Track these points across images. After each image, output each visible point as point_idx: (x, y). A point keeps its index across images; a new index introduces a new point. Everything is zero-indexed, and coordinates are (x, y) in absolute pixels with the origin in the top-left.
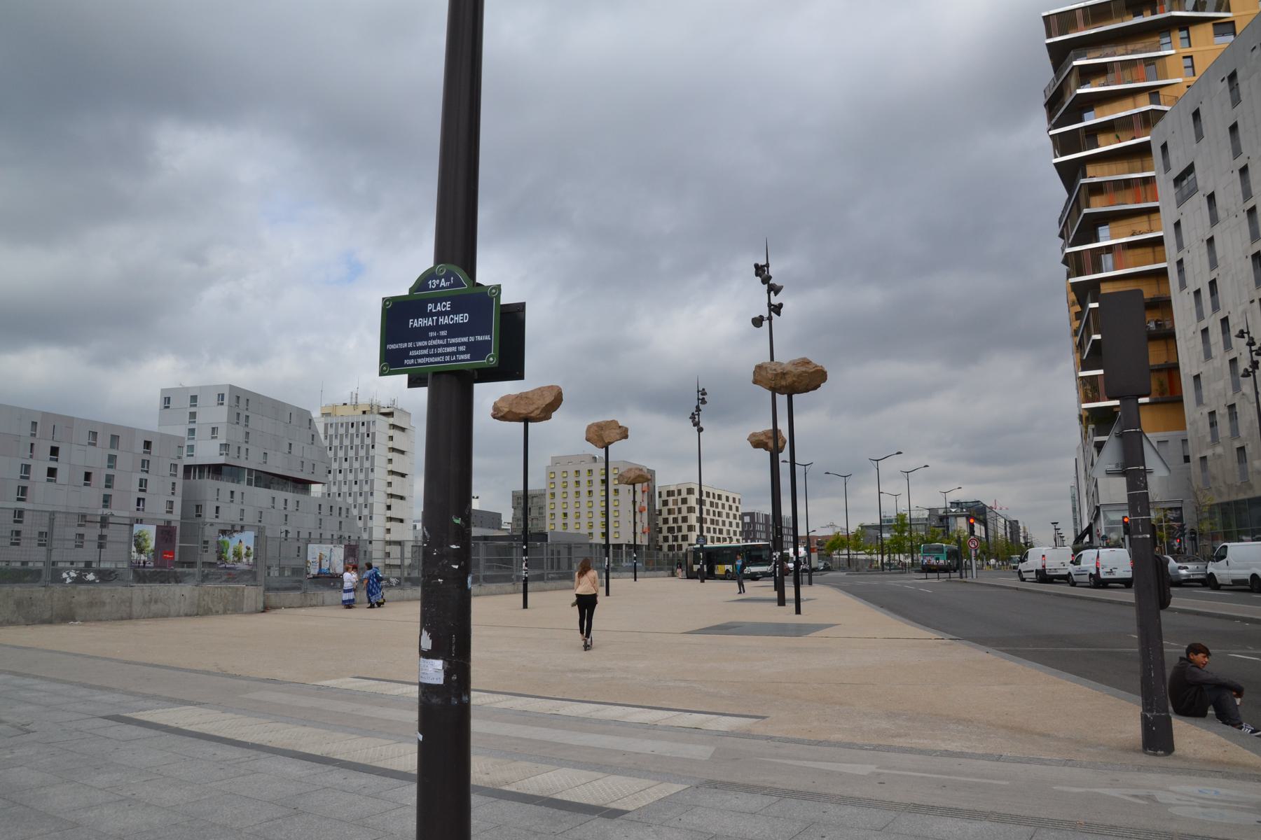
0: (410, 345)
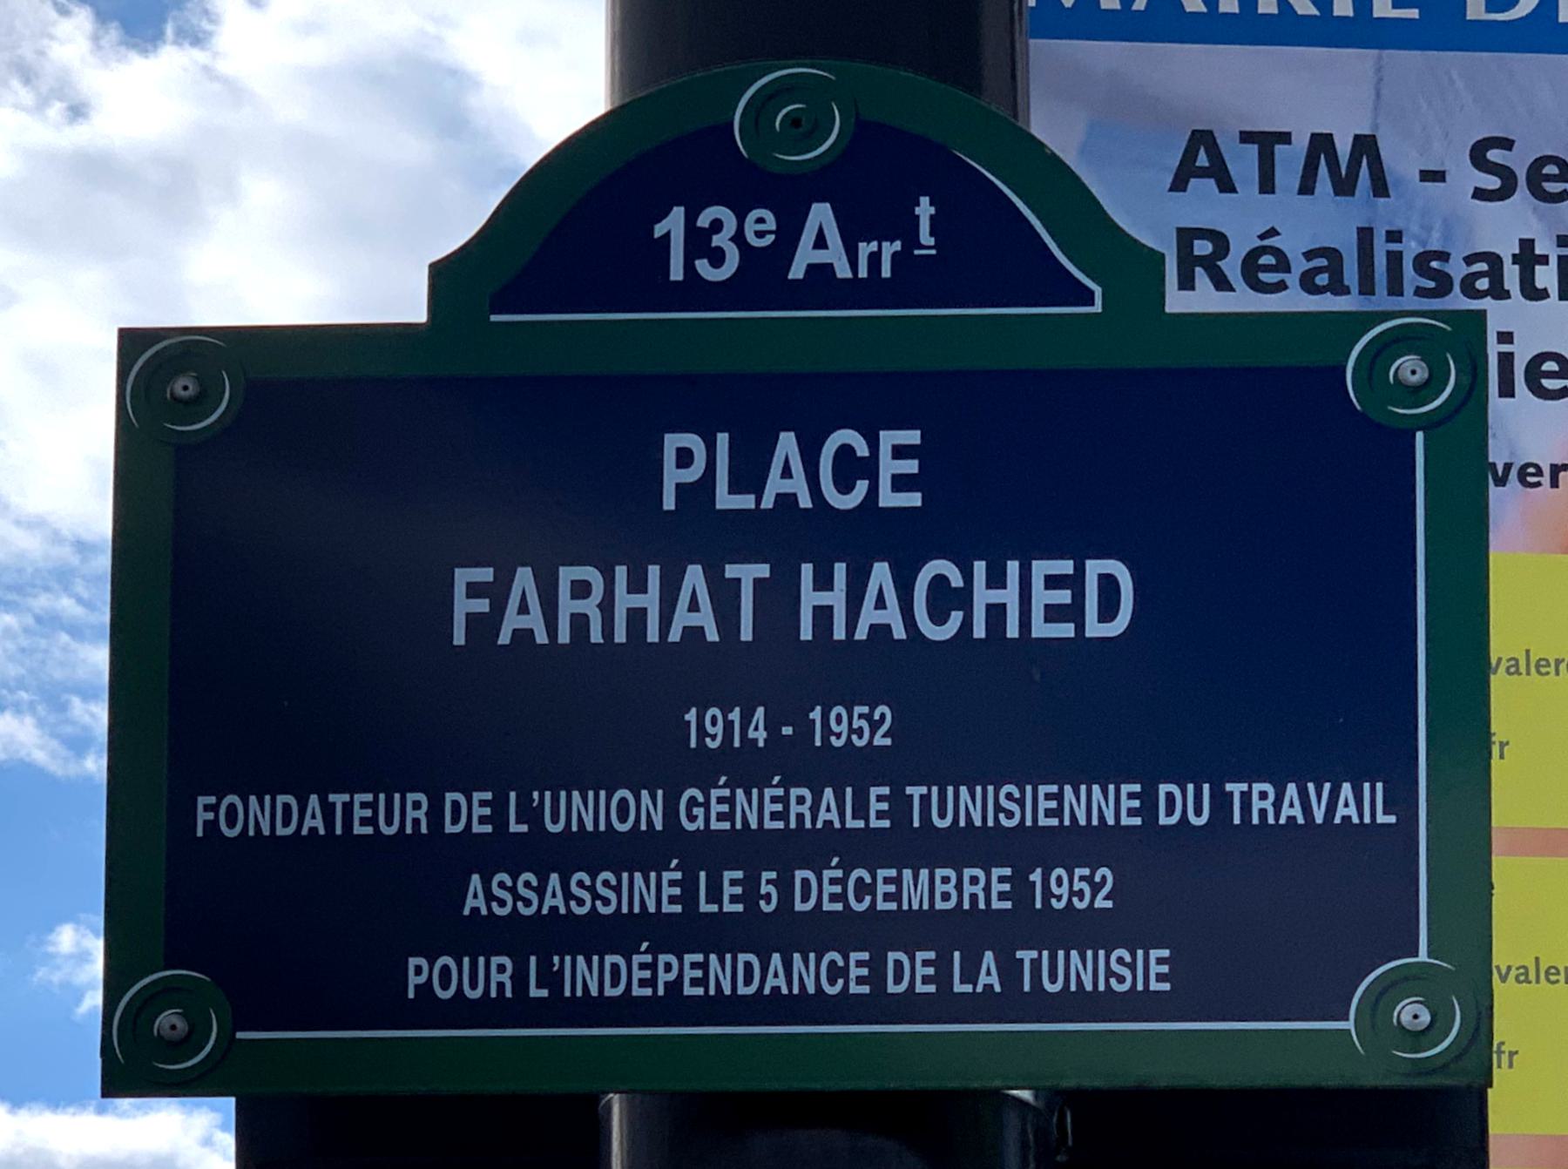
0: (470, 812)
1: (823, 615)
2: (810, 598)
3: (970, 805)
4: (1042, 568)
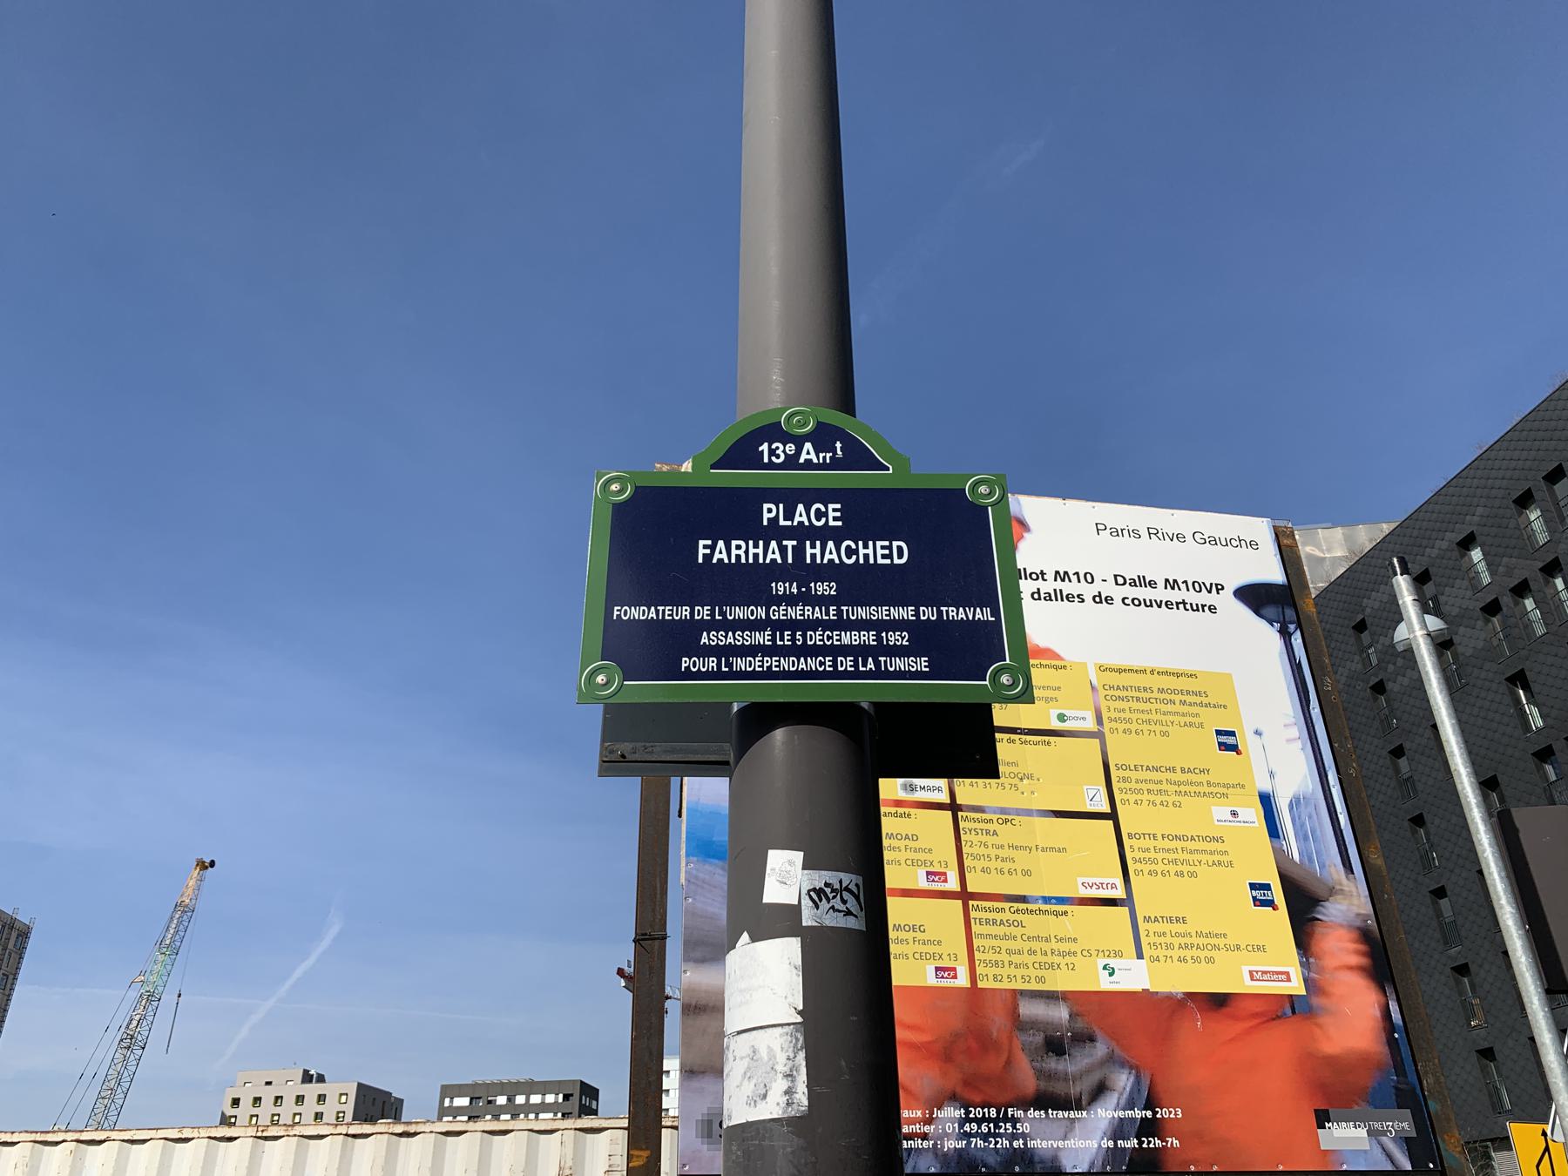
0: (703, 613)
1: (813, 556)
2: (809, 551)
3: (861, 613)
4: (879, 544)
